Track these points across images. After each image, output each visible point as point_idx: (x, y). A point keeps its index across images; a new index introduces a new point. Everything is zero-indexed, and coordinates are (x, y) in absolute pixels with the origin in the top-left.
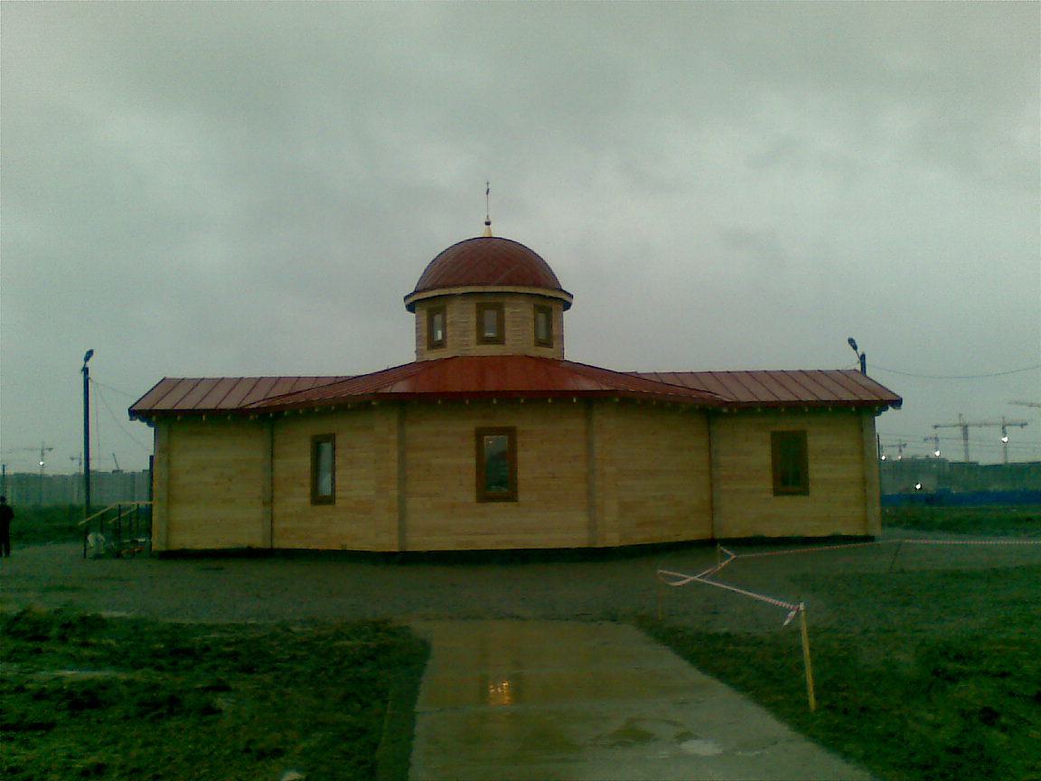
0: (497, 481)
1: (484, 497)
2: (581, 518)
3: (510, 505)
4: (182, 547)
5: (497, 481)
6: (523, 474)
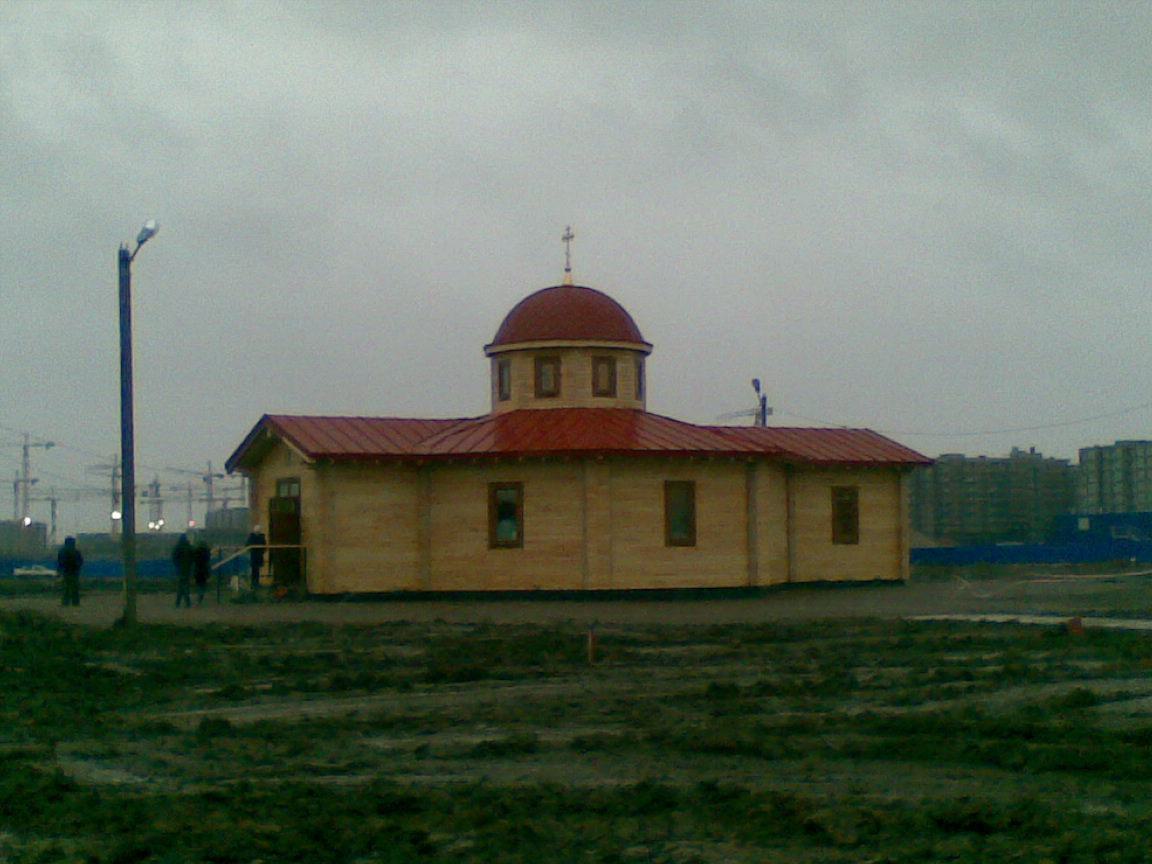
0: (681, 529)
1: (671, 542)
2: (741, 560)
3: (690, 549)
4: (344, 590)
5: (681, 529)
6: (701, 523)
